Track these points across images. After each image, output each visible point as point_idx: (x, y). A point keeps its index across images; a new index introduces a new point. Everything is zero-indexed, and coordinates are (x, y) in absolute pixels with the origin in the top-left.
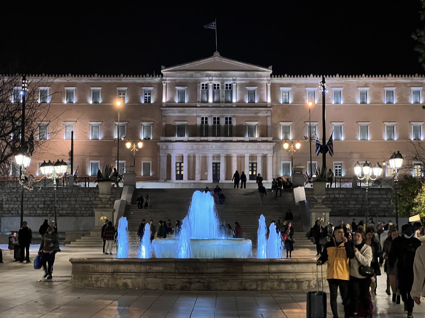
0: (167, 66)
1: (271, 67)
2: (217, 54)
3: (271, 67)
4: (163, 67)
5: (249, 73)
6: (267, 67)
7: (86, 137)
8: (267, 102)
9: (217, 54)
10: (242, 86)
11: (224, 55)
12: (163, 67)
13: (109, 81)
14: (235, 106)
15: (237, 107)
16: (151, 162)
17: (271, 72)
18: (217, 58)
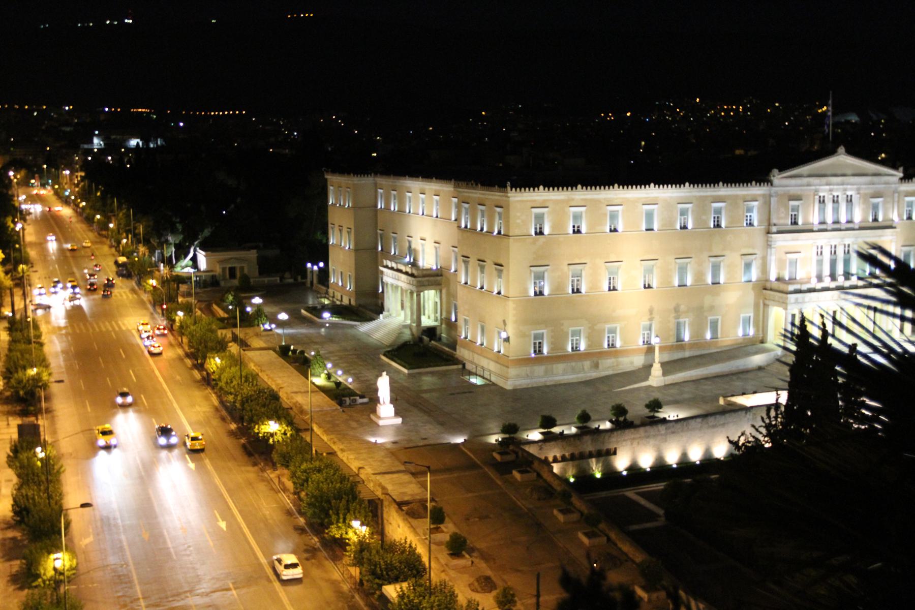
0: (782, 169)
1: (901, 169)
2: (841, 149)
3: (901, 169)
4: (775, 171)
5: (875, 179)
6: (895, 167)
7: (670, 282)
8: (892, 220)
9: (841, 149)
10: (866, 198)
11: (850, 152)
12: (775, 171)
13: (702, 194)
14: (857, 227)
15: (861, 228)
16: (752, 315)
17: (901, 175)
18: (842, 159)
